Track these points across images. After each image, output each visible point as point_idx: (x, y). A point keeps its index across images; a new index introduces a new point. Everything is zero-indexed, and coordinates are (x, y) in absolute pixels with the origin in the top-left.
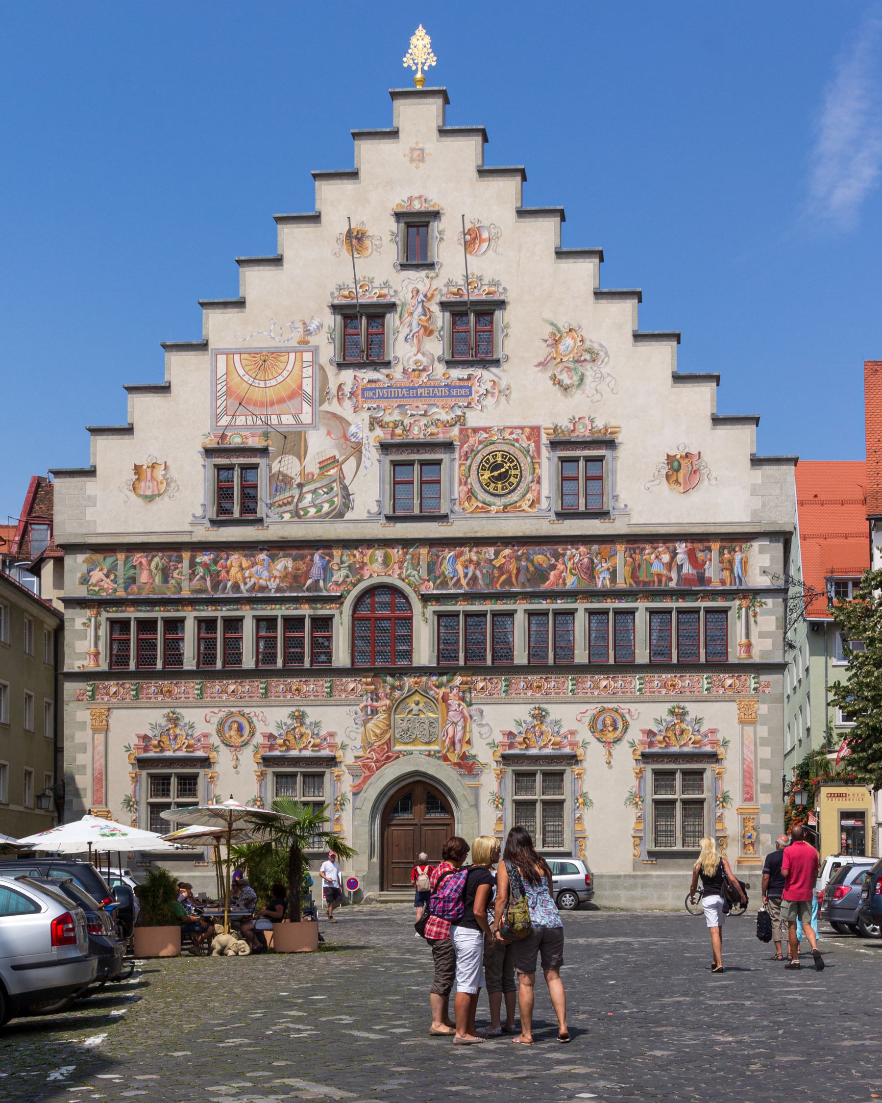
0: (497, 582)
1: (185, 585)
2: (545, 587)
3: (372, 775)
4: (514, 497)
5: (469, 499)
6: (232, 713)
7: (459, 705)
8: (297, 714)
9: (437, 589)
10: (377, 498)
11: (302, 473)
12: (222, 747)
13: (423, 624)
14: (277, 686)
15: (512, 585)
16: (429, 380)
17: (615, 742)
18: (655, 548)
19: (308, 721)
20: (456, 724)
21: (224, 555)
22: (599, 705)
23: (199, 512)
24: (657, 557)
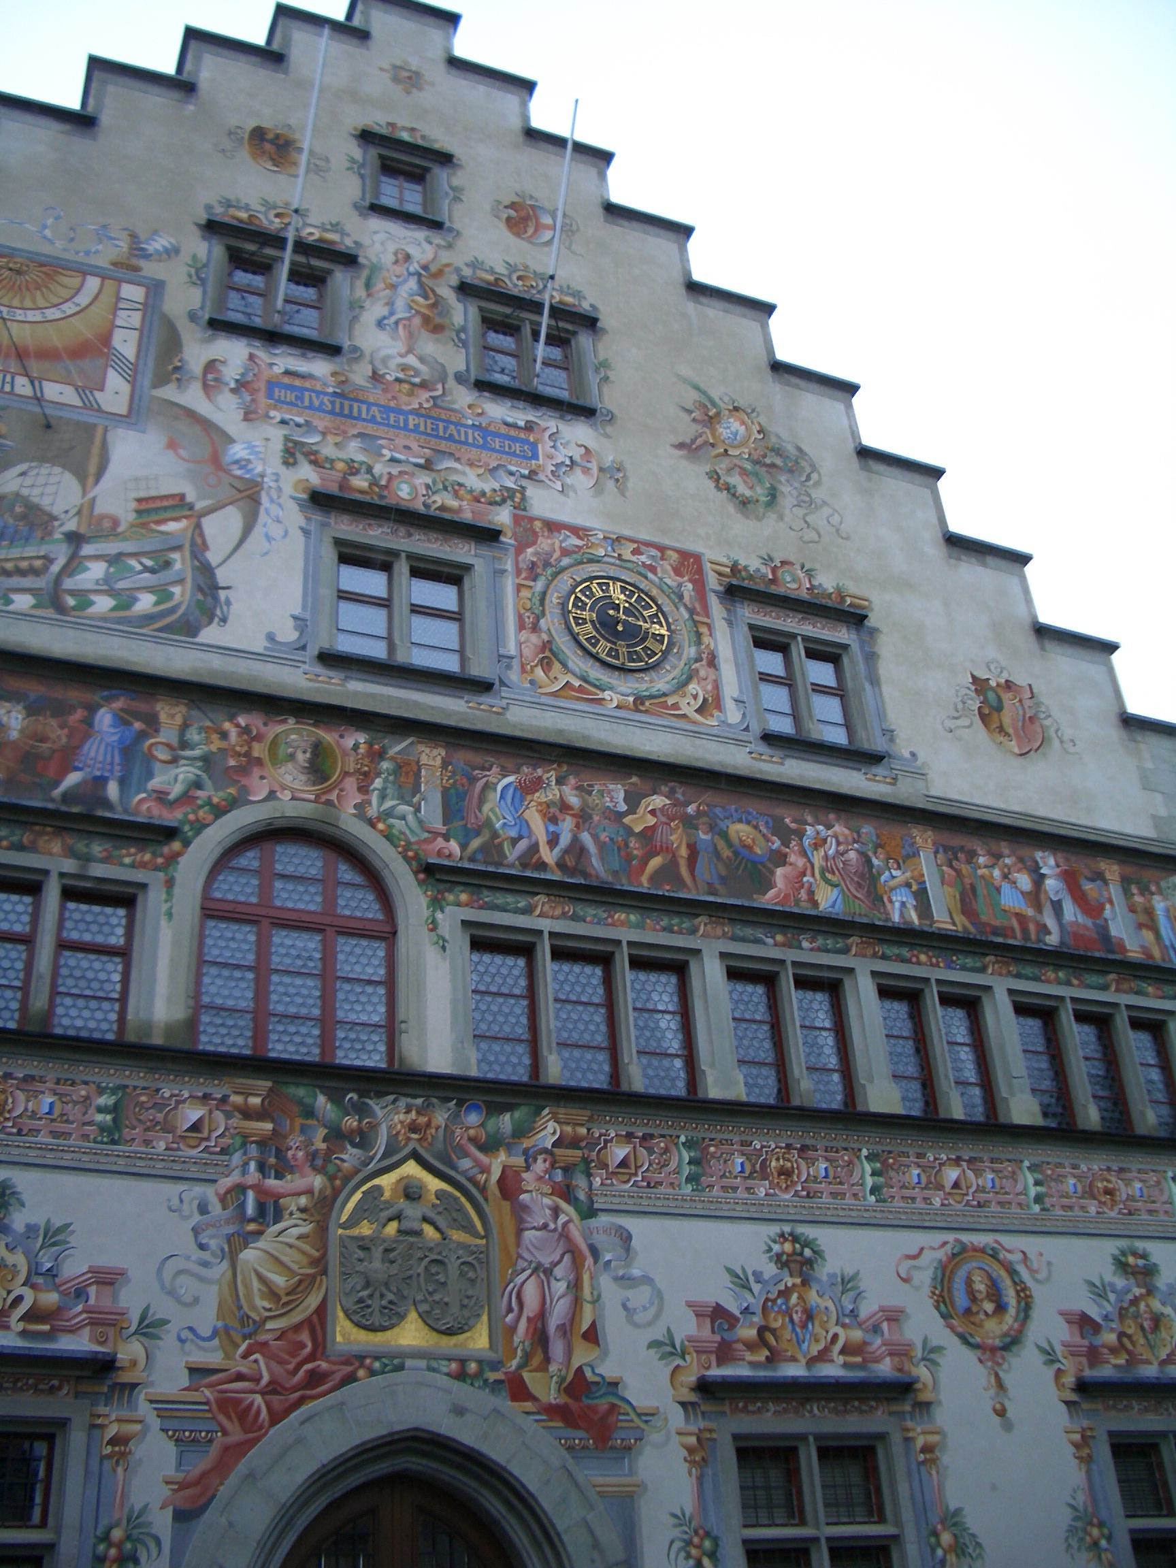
2: (769, 900)
3: (258, 1439)
4: (660, 682)
7: (556, 1211)
10: (297, 611)
11: (86, 510)
16: (435, 405)
17: (1006, 1348)
18: (997, 857)
20: (548, 1272)
22: (950, 1237)
24: (1005, 876)
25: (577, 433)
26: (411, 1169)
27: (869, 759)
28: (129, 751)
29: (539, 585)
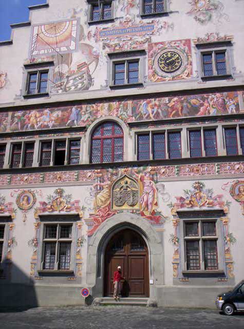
0: (170, 115)
1: (8, 127)
2: (198, 115)
4: (178, 73)
5: (154, 75)
6: (25, 191)
7: (150, 183)
8: (59, 191)
9: (137, 120)
10: (106, 79)
12: (19, 211)
13: (129, 139)
14: (50, 176)
15: (179, 115)
19: (64, 195)
21: (28, 112)
22: (235, 180)
23: (19, 93)
25: (164, 19)
26: (127, 179)
27: (228, 77)
28: (77, 115)
29: (153, 59)
